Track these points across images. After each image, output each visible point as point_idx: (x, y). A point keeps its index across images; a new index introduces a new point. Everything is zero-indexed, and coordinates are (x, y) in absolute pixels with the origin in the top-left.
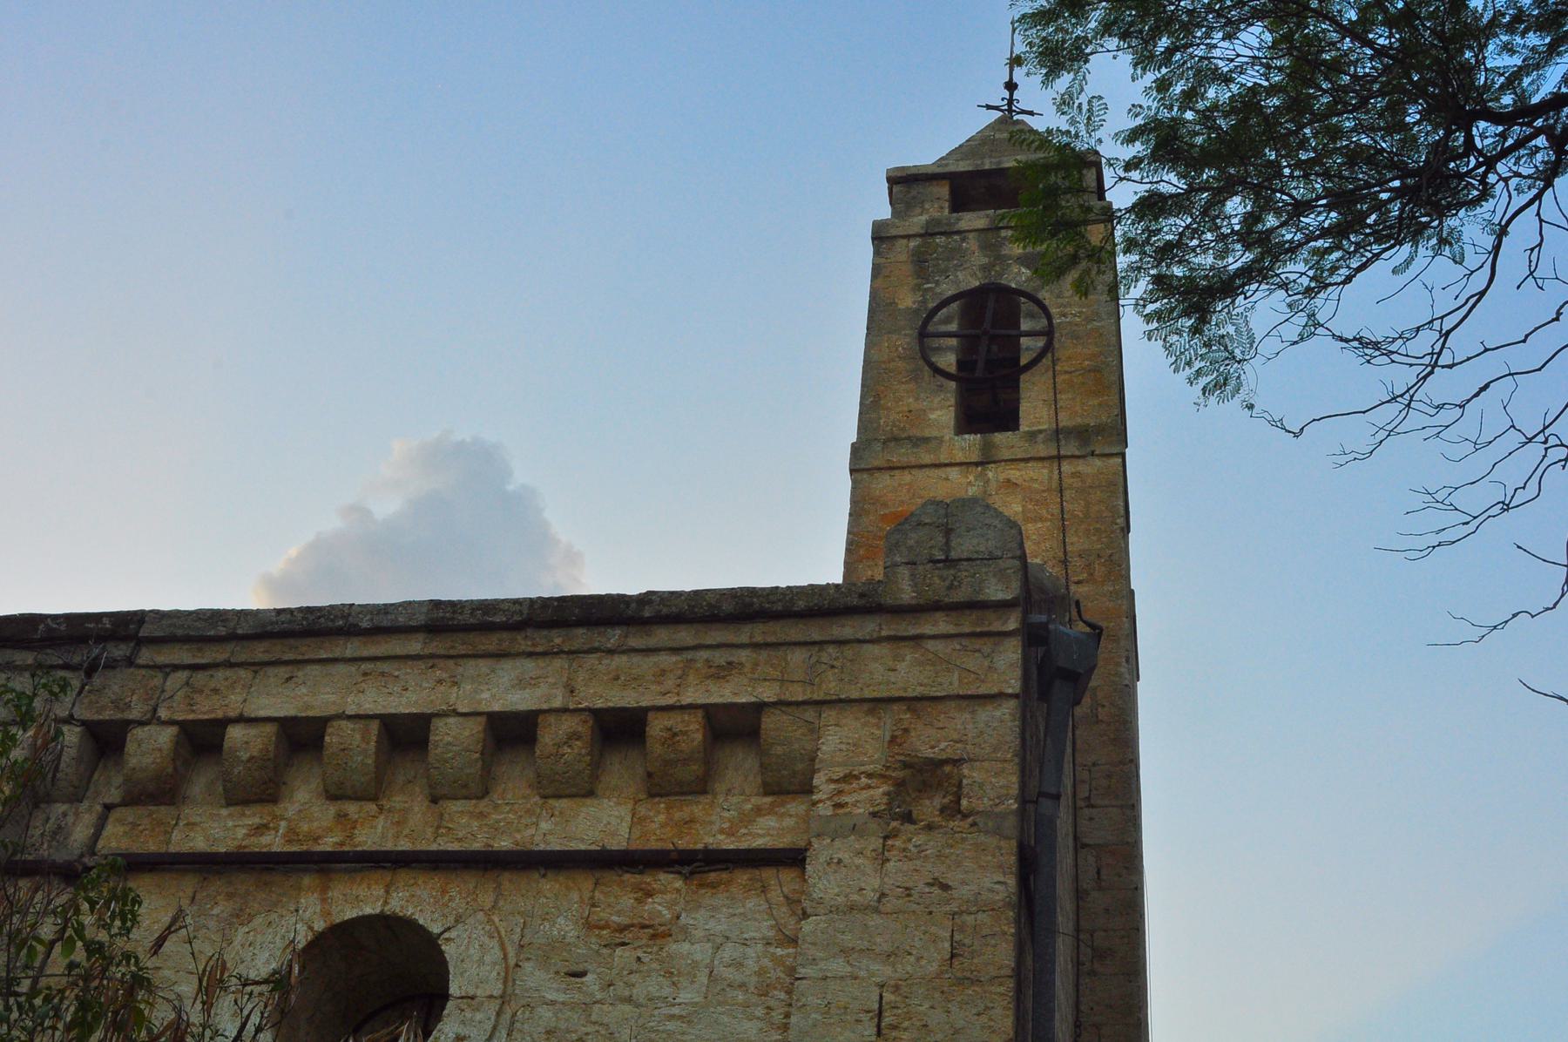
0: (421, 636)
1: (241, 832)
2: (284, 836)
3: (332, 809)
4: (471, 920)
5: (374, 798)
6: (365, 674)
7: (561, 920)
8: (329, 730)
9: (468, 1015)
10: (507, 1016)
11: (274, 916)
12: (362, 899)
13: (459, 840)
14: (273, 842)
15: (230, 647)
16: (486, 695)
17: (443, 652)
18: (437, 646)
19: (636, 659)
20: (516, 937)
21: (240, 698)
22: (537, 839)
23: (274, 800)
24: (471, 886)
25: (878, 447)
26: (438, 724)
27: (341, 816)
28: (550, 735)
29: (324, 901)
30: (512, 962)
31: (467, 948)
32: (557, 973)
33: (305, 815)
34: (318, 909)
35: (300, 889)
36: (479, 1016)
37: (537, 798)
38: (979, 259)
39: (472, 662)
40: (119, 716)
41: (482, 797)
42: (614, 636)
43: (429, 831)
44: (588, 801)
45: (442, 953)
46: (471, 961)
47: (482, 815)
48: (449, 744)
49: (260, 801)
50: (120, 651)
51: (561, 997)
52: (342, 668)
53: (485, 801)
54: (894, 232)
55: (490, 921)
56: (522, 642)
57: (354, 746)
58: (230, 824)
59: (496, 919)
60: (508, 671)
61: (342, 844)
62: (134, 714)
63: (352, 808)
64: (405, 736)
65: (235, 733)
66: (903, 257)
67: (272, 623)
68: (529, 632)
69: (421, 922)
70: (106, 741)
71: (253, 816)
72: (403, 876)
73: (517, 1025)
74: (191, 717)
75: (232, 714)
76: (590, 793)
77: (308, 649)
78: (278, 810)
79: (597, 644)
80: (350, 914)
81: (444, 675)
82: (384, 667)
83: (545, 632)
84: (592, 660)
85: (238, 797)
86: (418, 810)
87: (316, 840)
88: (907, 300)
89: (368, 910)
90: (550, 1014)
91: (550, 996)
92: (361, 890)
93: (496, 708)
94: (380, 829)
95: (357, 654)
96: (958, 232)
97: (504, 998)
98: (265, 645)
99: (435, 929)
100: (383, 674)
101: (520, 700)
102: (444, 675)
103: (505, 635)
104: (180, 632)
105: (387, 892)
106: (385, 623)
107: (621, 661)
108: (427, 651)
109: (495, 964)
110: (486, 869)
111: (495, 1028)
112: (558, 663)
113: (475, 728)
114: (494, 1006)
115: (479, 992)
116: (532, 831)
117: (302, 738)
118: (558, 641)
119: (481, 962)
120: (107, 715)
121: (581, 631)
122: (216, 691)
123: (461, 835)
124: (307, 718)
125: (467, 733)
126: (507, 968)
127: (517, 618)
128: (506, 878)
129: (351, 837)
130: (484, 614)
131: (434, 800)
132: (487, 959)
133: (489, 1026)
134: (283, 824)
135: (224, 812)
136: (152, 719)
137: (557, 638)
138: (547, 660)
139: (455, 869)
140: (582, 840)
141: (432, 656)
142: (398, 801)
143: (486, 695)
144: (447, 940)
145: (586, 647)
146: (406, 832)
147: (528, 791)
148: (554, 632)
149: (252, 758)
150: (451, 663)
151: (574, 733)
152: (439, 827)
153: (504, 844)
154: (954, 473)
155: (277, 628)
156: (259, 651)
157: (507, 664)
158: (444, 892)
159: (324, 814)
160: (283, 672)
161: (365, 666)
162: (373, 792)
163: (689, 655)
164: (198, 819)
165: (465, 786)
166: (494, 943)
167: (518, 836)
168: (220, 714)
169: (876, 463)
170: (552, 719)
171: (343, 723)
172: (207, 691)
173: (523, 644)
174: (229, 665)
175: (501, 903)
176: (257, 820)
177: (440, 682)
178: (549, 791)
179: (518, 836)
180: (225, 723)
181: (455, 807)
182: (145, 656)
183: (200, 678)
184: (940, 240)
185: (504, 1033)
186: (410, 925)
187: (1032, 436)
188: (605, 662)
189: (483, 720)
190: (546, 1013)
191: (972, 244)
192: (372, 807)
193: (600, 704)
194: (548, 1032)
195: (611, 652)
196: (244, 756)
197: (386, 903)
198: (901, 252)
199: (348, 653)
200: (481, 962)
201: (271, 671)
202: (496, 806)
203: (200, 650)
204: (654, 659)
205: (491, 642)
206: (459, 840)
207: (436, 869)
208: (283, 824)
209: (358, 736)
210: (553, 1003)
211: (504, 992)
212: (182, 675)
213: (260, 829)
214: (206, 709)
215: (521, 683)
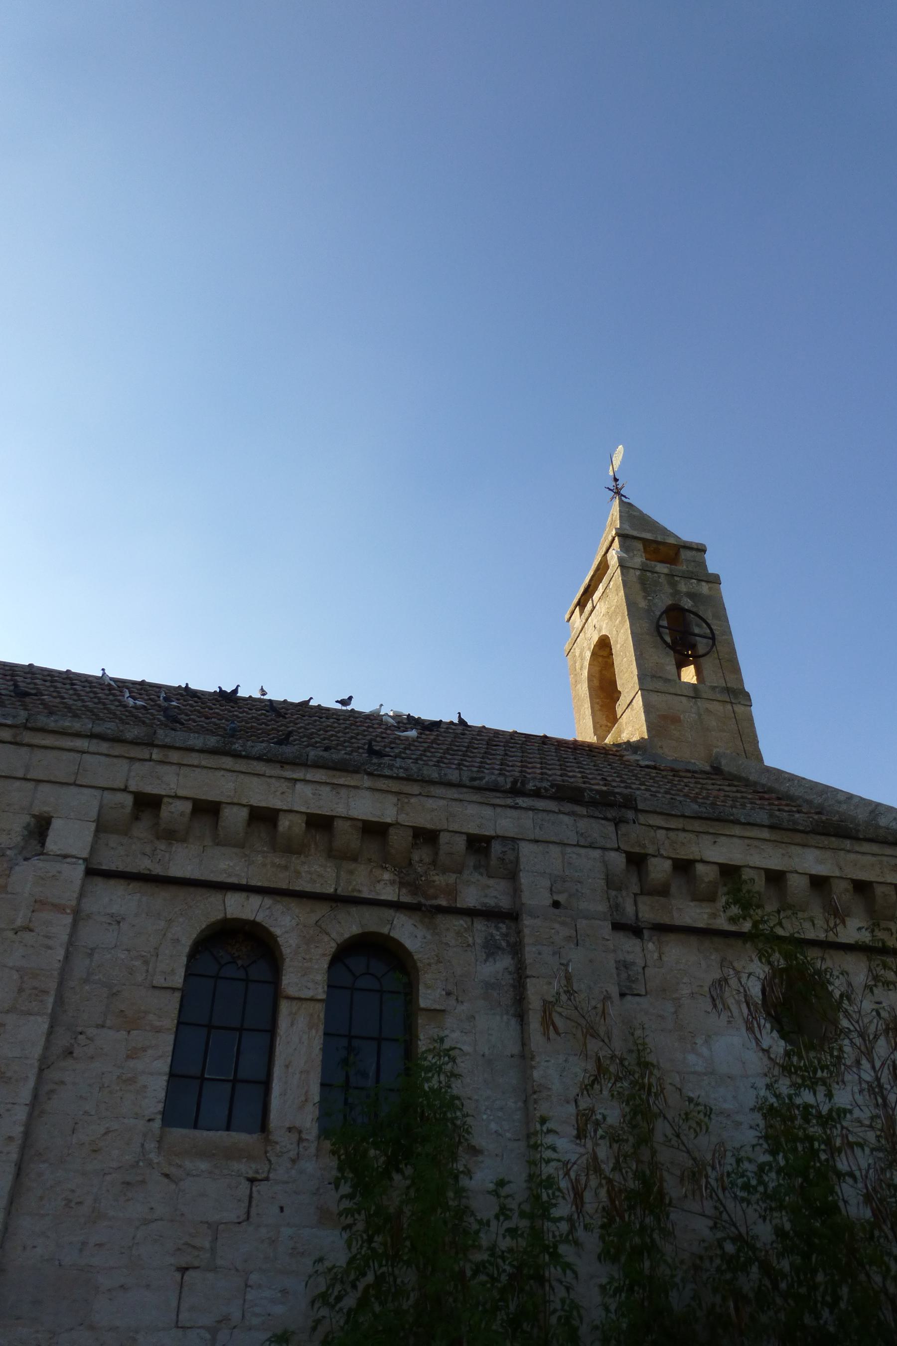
0: (766, 830)
15: (681, 820)
19: (859, 856)
38: (668, 589)
39: (793, 847)
40: (643, 851)
42: (848, 844)
50: (630, 814)
52: (735, 840)
58: (698, 911)
62: (651, 850)
65: (700, 868)
66: (635, 579)
70: (637, 861)
74: (678, 857)
75: (698, 858)
82: (756, 843)
95: (742, 835)
96: (656, 573)
104: (658, 810)
106: (751, 821)
107: (852, 856)
108: (772, 839)
118: (826, 842)
120: (637, 850)
121: (833, 839)
135: (692, 904)
136: (658, 855)
141: (775, 841)
148: (823, 837)
154: (684, 699)
156: (697, 825)
161: (747, 841)
163: (880, 858)
168: (691, 857)
169: (651, 688)
174: (684, 830)
182: (642, 818)
183: (672, 834)
184: (649, 574)
187: (713, 688)
191: (662, 579)
195: (849, 851)
196: (706, 880)
198: (634, 575)
205: (799, 838)
212: (663, 832)
214: (684, 854)
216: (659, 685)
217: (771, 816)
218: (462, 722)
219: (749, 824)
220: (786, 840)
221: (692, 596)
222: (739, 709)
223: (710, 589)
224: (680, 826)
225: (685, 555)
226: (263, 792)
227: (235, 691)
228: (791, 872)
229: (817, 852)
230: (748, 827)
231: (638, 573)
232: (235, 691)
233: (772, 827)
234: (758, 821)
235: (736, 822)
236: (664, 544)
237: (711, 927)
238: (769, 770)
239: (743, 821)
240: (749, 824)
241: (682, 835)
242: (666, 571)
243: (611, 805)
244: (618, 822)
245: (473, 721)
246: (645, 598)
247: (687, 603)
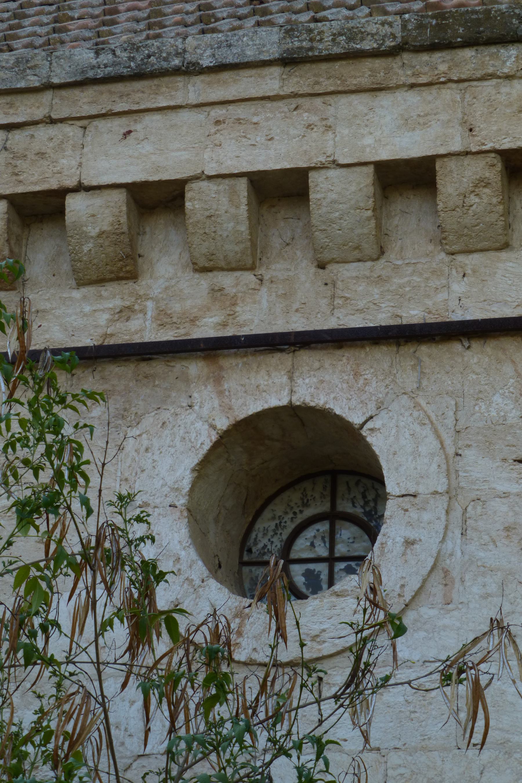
0: (276, 71)
1: (103, 318)
2: (155, 319)
3: (205, 282)
4: (395, 406)
5: (252, 268)
6: (217, 122)
7: (497, 399)
8: (188, 195)
9: (413, 514)
10: (457, 513)
11: (165, 415)
12: (264, 388)
13: (360, 311)
14: (144, 329)
15: (47, 96)
16: (369, 141)
17: (306, 90)
18: (299, 80)
20: (450, 421)
21: (74, 163)
22: (453, 304)
23: (133, 276)
24: (386, 366)
26: (314, 177)
27: (217, 292)
28: (452, 182)
29: (221, 393)
30: (451, 451)
31: (397, 438)
32: (504, 460)
33: (172, 295)
34: (216, 403)
35: (187, 381)
36: (426, 516)
37: (443, 255)
39: (343, 100)
41: (378, 259)
43: (324, 302)
44: (503, 255)
45: (368, 447)
46: (403, 452)
47: (380, 280)
48: (334, 202)
49: (119, 279)
51: (514, 488)
52: (185, 115)
53: (382, 261)
55: (417, 405)
56: (401, 69)
57: (221, 211)
58: (87, 309)
59: (423, 403)
60: (388, 109)
61: (224, 325)
63: (226, 280)
64: (280, 192)
65: (75, 205)
67: (93, 68)
68: (406, 57)
69: (338, 412)
71: (114, 296)
72: (306, 358)
73: (469, 522)
74: (20, 189)
75: (70, 182)
76: (506, 246)
77: (141, 95)
78: (142, 286)
79: (491, 70)
80: (254, 407)
81: (314, 119)
83: (425, 57)
84: (488, 86)
85: (91, 277)
86: (305, 273)
87: (193, 321)
89: (275, 401)
90: (505, 508)
91: (502, 487)
92: (261, 378)
93: (384, 155)
94: (265, 304)
97: (451, 494)
98: (90, 92)
99: (356, 419)
100: (239, 121)
101: (409, 146)
102: (314, 119)
103: (378, 63)
105: (291, 379)
106: (230, 59)
108: (287, 90)
109: (433, 455)
110: (398, 345)
111: (446, 528)
112: (449, 94)
113: (364, 181)
114: (442, 503)
115: (421, 489)
116: (442, 296)
117: (157, 201)
118: (443, 68)
119: (416, 454)
121: (468, 53)
122: (41, 155)
123: (361, 304)
124: (160, 183)
125: (353, 188)
126: (446, 458)
127: (390, 43)
128: (424, 349)
129: (233, 315)
130: (350, 39)
131: (322, 266)
132: (423, 449)
133: (440, 526)
134: (150, 304)
135: (77, 294)
137: (440, 62)
138: (434, 90)
139: (363, 347)
140: (506, 303)
141: (295, 95)
142: (277, 269)
143: (369, 141)
144: (372, 430)
145: (479, 74)
146: (296, 306)
147: (431, 247)
148: (437, 56)
149: (101, 234)
150: (318, 101)
151: (481, 180)
152: (333, 297)
153: (414, 314)
155: (100, 74)
156: (85, 101)
157: (385, 100)
158: (357, 375)
159: (195, 290)
160: (118, 125)
161: (218, 112)
162: (250, 260)
164: (48, 306)
165: (358, 248)
166: (427, 431)
167: (429, 303)
168: (53, 184)
170: (452, 164)
171: (204, 184)
172: (31, 156)
173: (404, 76)
175: (425, 383)
176: (117, 303)
177: (310, 127)
178: (455, 248)
179: (429, 303)
180: (62, 193)
181: (347, 272)
185: (458, 532)
186: (324, 415)
188: (504, 90)
189: (370, 169)
190: (500, 507)
192: (248, 277)
193: (507, 144)
194: (507, 529)
195: (509, 77)
196: (93, 232)
197: (292, 391)
199: (193, 98)
200: (416, 454)
201: (101, 124)
202: (397, 267)
203: (11, 105)
205: (363, 72)
206: (360, 311)
207: (340, 347)
208: (150, 304)
209: (224, 200)
210: (506, 495)
211: (449, 485)
213: (125, 313)
214: (35, 180)
215: (407, 123)
217: (290, 30)
219: (221, 68)
224: (39, 114)
226: (394, 126)
228: (196, 178)
229: (412, 98)
230: (226, 75)
233: (289, 61)
234: (251, 54)
235: (191, 70)
237: (112, 341)
239: (206, 62)
240: (221, 68)
241: (43, 133)
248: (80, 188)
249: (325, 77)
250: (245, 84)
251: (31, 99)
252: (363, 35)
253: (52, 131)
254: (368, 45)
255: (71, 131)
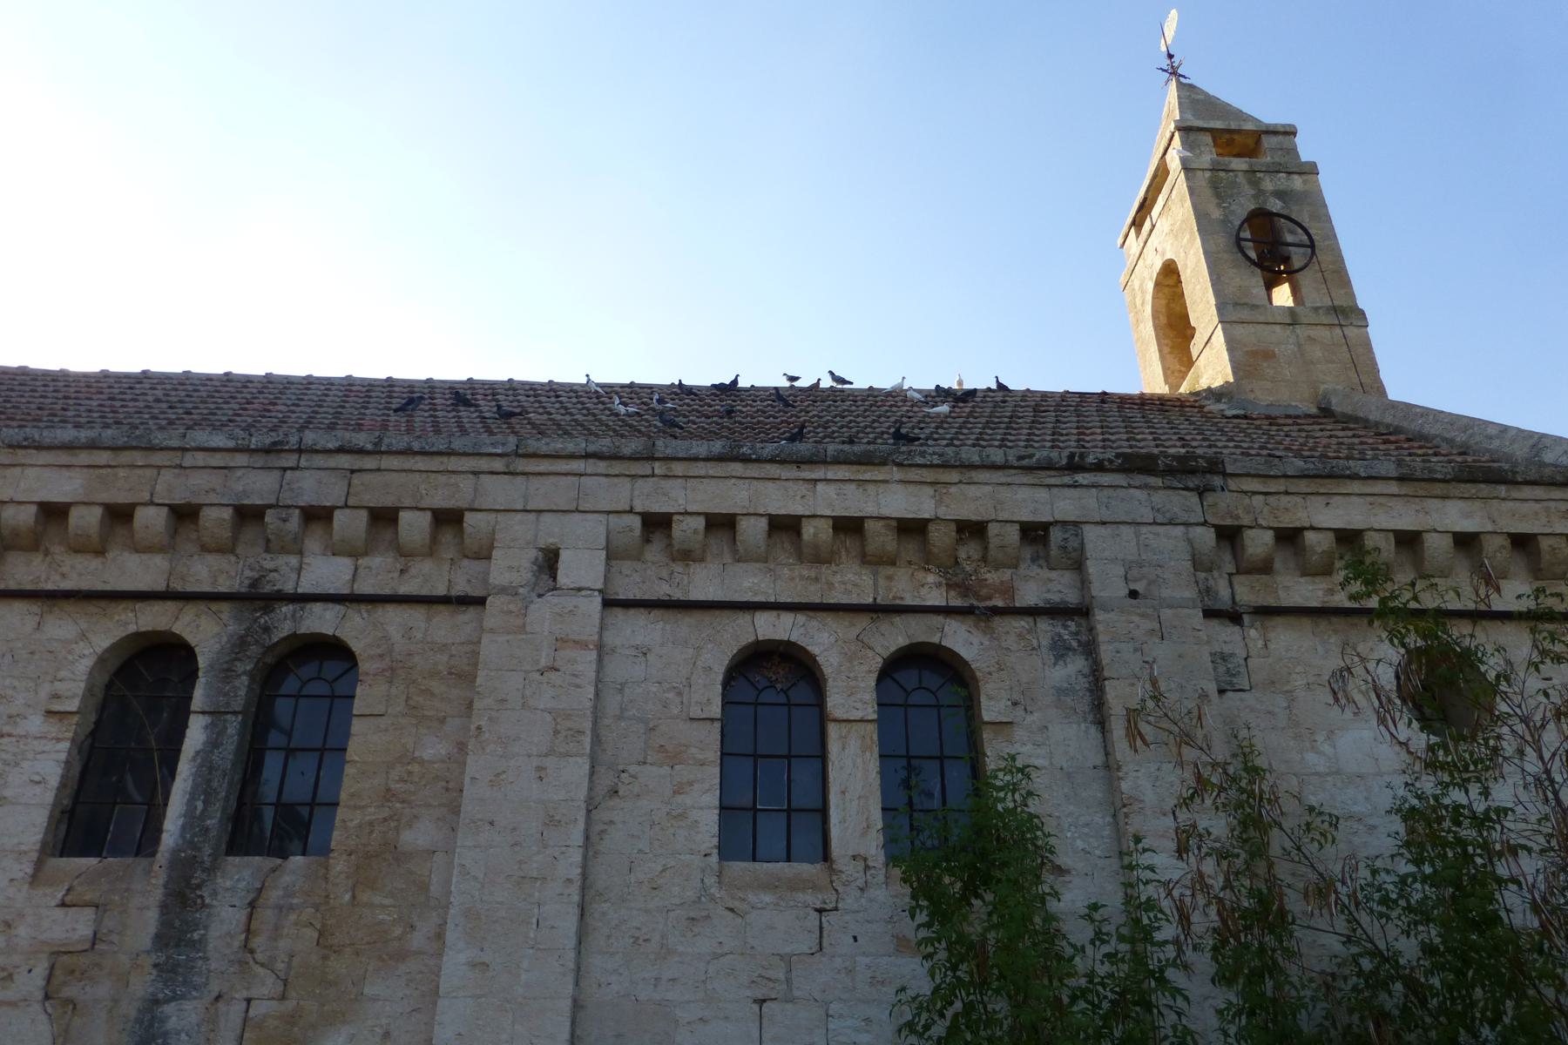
19: (1518, 504)
25: (1230, 308)
38: (1248, 190)
42: (1502, 490)
50: (1217, 481)
54: (1194, 166)
62: (1246, 521)
70: (1229, 535)
88: (1216, 214)
120: (1228, 522)
135: (1302, 580)
137: (1472, 489)
154: (1277, 328)
156: (1303, 485)
157: (1449, 503)
163: (1545, 504)
168: (1298, 524)
174: (1287, 493)
183: (1271, 499)
184: (1222, 174)
187: (1316, 309)
191: (1241, 179)
204: (1527, 505)
205: (1438, 489)
212: (1261, 497)
213: (1331, 592)
214: (1287, 521)
216: (1245, 314)
217: (1399, 463)
218: (1001, 387)
220: (1421, 493)
221: (1280, 195)
222: (1351, 332)
223: (1305, 182)
224: (1282, 489)
225: (1268, 142)
227: (735, 382)
229: (1461, 504)
231: (1208, 174)
232: (735, 382)
233: (1401, 479)
234: (1383, 473)
235: (1355, 477)
236: (1239, 132)
238: (1395, 405)
241: (1284, 499)
242: (1244, 167)
243: (1193, 472)
244: (1202, 492)
245: (1015, 384)
246: (1219, 205)
247: (1275, 205)
248: (1312, 528)
249: (1421, 489)
250: (1379, 487)
251: (1275, 481)
252: (1436, 472)
253: (1288, 498)
254: (1439, 476)
255: (1298, 499)
